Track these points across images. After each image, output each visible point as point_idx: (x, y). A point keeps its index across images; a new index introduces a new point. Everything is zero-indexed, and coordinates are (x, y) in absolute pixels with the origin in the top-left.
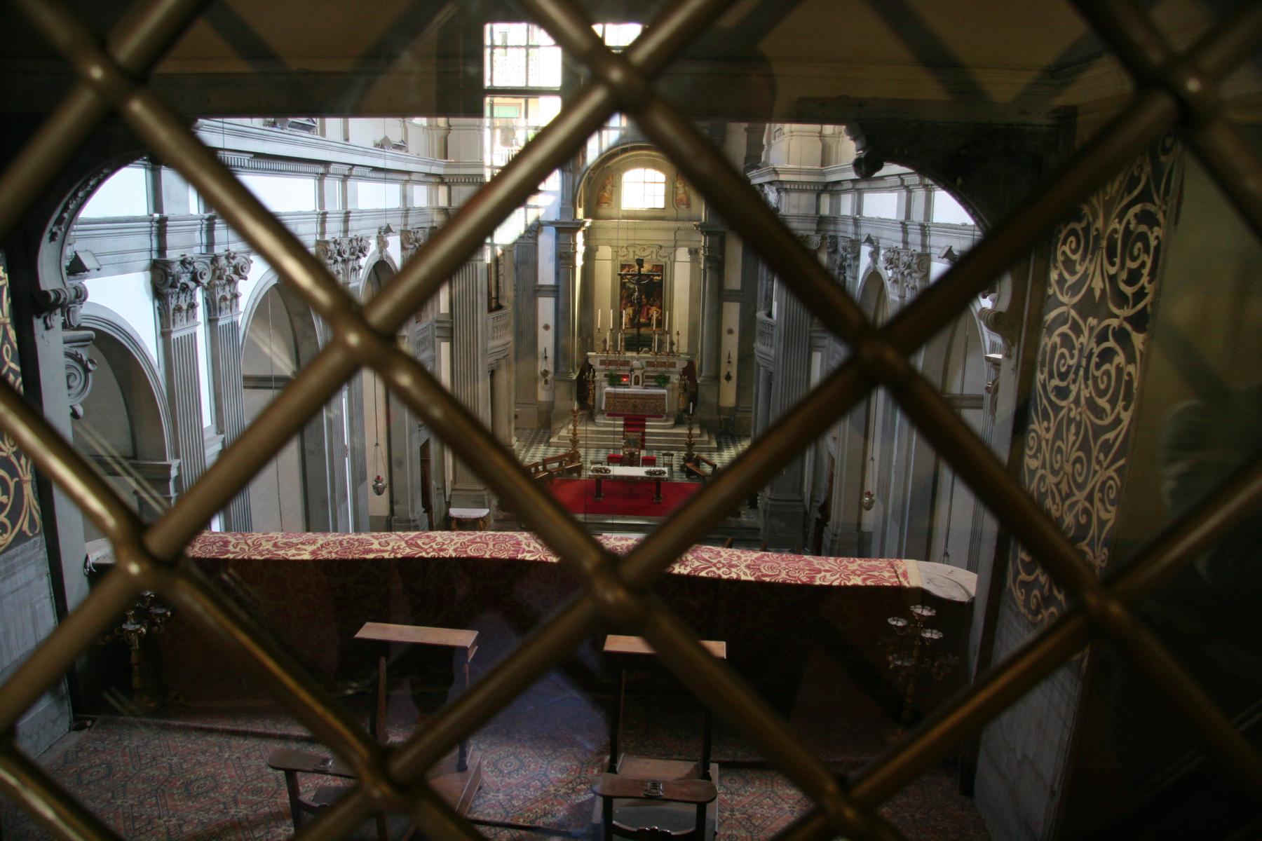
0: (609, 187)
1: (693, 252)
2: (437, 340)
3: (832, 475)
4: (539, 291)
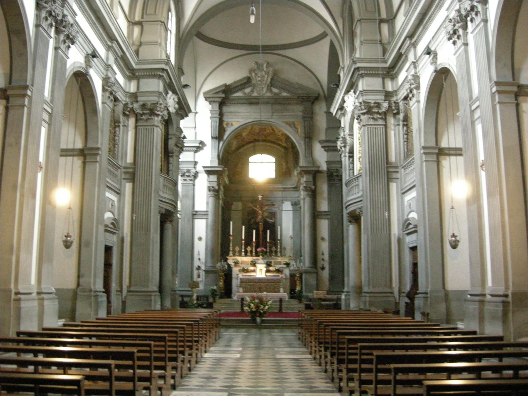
0: (240, 165)
1: (295, 205)
2: (123, 181)
3: (415, 265)
4: (195, 215)
